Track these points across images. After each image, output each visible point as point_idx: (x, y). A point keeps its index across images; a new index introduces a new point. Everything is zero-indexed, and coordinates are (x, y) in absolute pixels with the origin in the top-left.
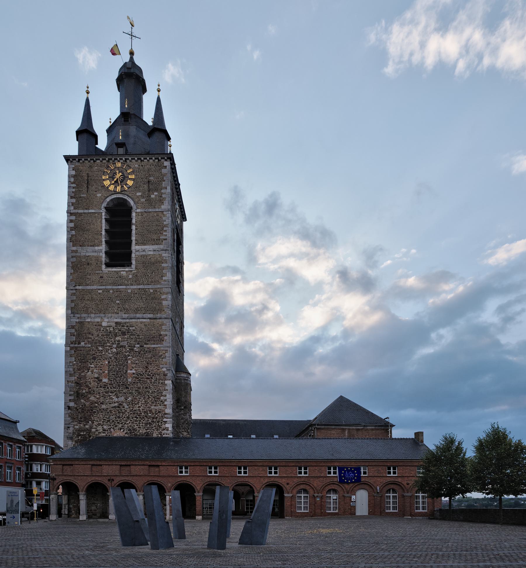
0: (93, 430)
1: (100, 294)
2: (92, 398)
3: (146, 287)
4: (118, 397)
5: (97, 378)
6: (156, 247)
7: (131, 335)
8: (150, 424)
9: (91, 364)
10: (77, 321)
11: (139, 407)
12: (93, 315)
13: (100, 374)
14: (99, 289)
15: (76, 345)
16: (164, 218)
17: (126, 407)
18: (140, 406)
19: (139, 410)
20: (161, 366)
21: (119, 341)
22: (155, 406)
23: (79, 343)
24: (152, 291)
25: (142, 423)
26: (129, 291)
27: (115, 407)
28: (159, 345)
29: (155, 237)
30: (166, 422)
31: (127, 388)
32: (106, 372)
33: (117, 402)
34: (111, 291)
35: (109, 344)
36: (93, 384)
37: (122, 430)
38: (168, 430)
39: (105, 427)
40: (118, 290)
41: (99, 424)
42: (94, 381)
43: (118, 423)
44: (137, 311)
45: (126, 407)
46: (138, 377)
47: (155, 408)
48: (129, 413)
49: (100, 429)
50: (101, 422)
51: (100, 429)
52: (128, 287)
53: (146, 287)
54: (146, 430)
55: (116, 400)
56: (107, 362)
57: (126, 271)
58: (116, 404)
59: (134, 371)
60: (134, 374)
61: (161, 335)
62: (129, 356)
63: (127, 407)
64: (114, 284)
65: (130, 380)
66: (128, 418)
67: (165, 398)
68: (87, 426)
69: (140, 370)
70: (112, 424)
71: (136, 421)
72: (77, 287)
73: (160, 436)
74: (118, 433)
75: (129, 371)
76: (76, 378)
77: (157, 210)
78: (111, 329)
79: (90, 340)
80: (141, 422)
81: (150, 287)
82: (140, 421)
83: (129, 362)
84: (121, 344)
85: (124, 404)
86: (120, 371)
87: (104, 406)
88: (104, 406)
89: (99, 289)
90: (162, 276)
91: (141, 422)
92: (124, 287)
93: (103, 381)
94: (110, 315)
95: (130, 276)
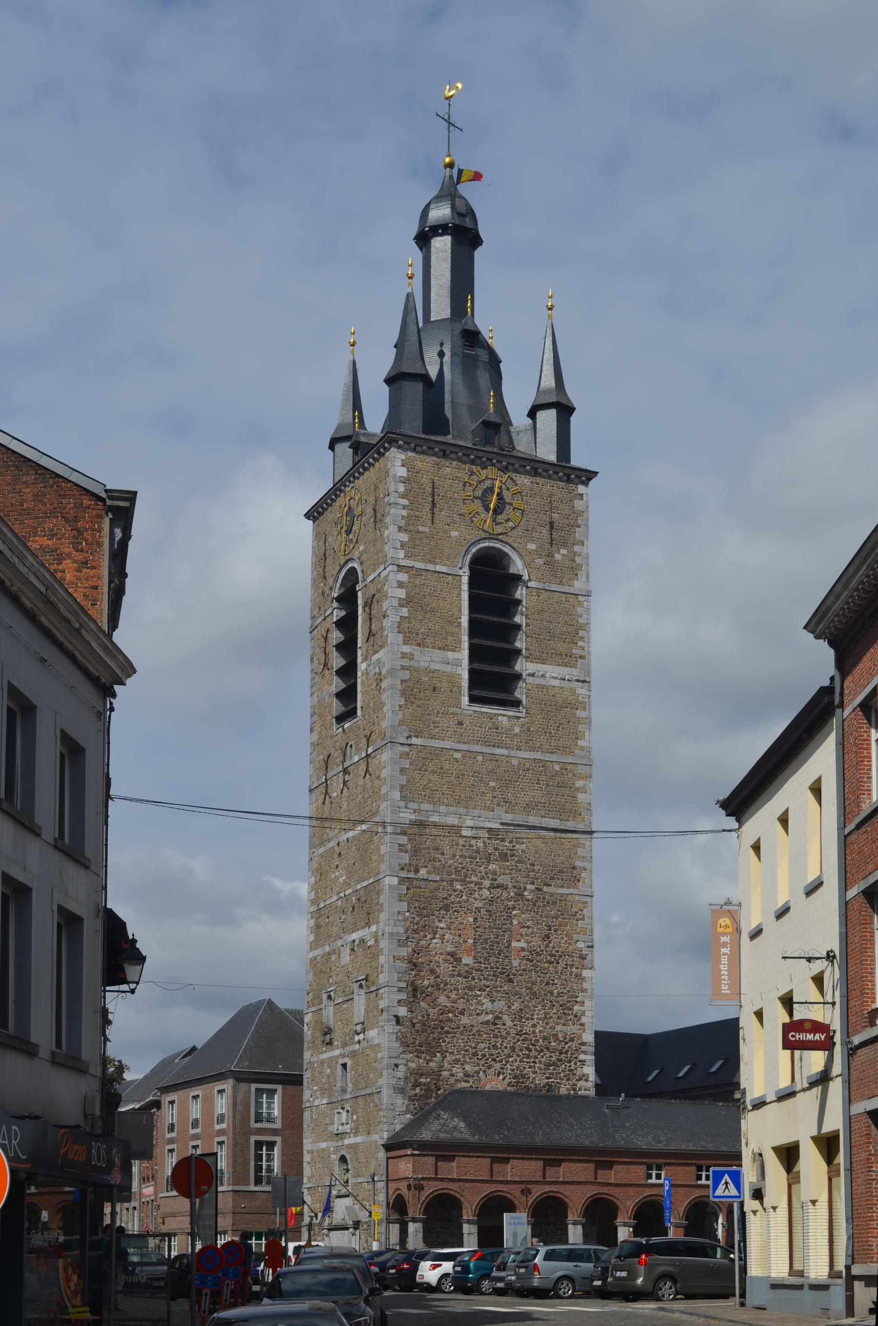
0: (445, 1074)
1: (457, 760)
2: (442, 1000)
3: (548, 757)
4: (493, 1001)
5: (452, 954)
6: (564, 671)
7: (518, 862)
8: (554, 1064)
9: (440, 921)
10: (413, 817)
11: (534, 1026)
12: (443, 809)
13: (457, 945)
14: (456, 750)
15: (412, 875)
16: (579, 610)
17: (509, 1023)
18: (535, 1026)
19: (534, 1032)
20: (575, 937)
21: (494, 873)
22: (564, 1025)
23: (417, 871)
24: (557, 767)
25: (540, 1062)
26: (515, 762)
27: (487, 1023)
28: (571, 891)
29: (562, 648)
30: (583, 1062)
31: (511, 981)
32: (471, 941)
33: (492, 1012)
34: (480, 758)
35: (474, 879)
36: (444, 969)
37: (501, 1077)
38: (587, 1080)
39: (468, 1068)
40: (493, 757)
41: (457, 1061)
42: (446, 961)
43: (494, 1060)
44: (529, 807)
45: (509, 1023)
46: (532, 956)
47: (564, 1028)
48: (514, 1038)
49: (458, 1071)
50: (461, 1056)
51: (458, 1071)
52: (513, 753)
53: (548, 757)
54: (547, 1078)
55: (487, 1005)
56: (471, 920)
57: (509, 717)
58: (490, 1017)
59: (524, 945)
60: (523, 949)
61: (574, 868)
62: (514, 908)
63: (511, 1024)
64: (486, 743)
65: (515, 963)
66: (513, 1049)
67: (582, 1008)
68: (432, 1065)
69: (536, 942)
70: (482, 1062)
71: (528, 1056)
72: (414, 740)
73: (572, 1092)
74: (494, 1083)
75: (514, 944)
76: (410, 950)
77: (566, 589)
78: (480, 844)
79: (437, 864)
80: (537, 1061)
81: (554, 758)
82: (536, 1058)
83: (515, 922)
84: (501, 880)
85: (505, 1017)
86: (498, 943)
87: (465, 1020)
88: (465, 1020)
89: (456, 750)
90: (577, 738)
91: (537, 1061)
92: (504, 752)
93: (464, 961)
94: (476, 812)
95: (517, 730)
